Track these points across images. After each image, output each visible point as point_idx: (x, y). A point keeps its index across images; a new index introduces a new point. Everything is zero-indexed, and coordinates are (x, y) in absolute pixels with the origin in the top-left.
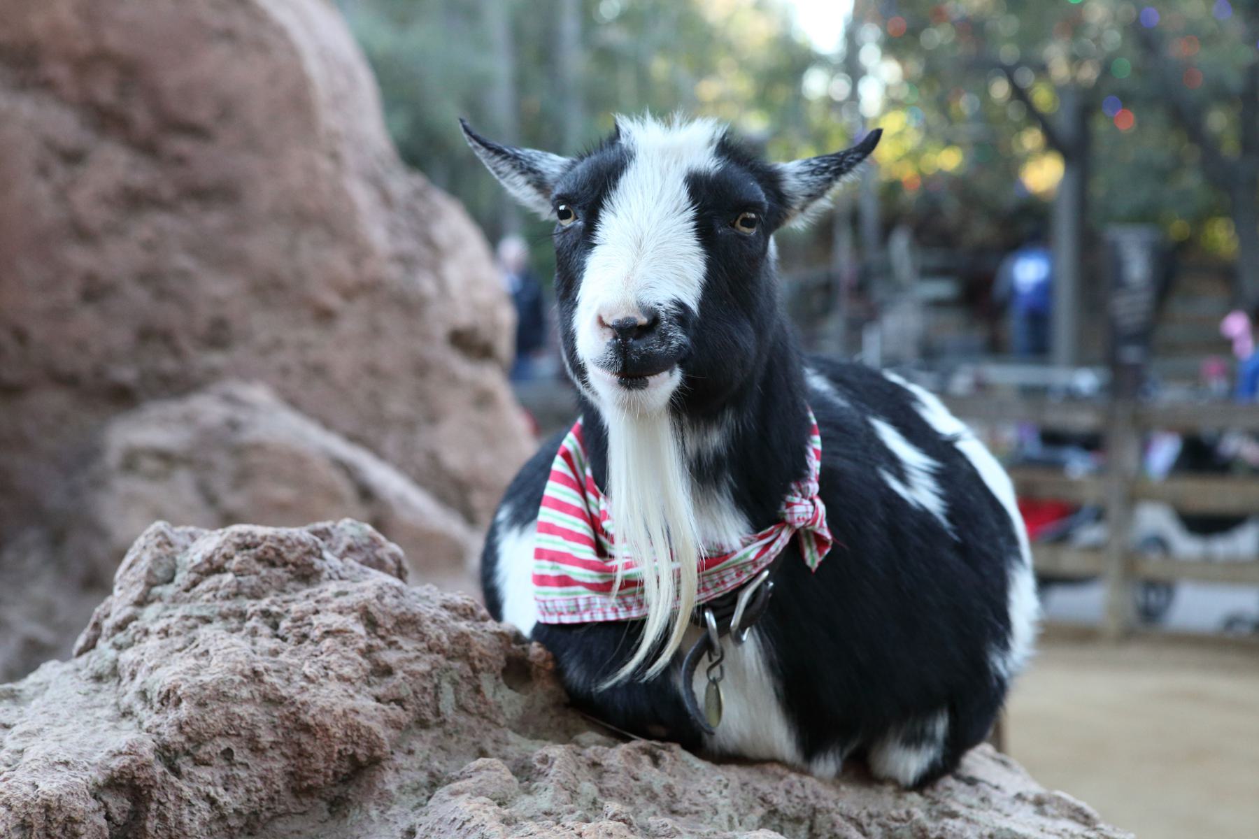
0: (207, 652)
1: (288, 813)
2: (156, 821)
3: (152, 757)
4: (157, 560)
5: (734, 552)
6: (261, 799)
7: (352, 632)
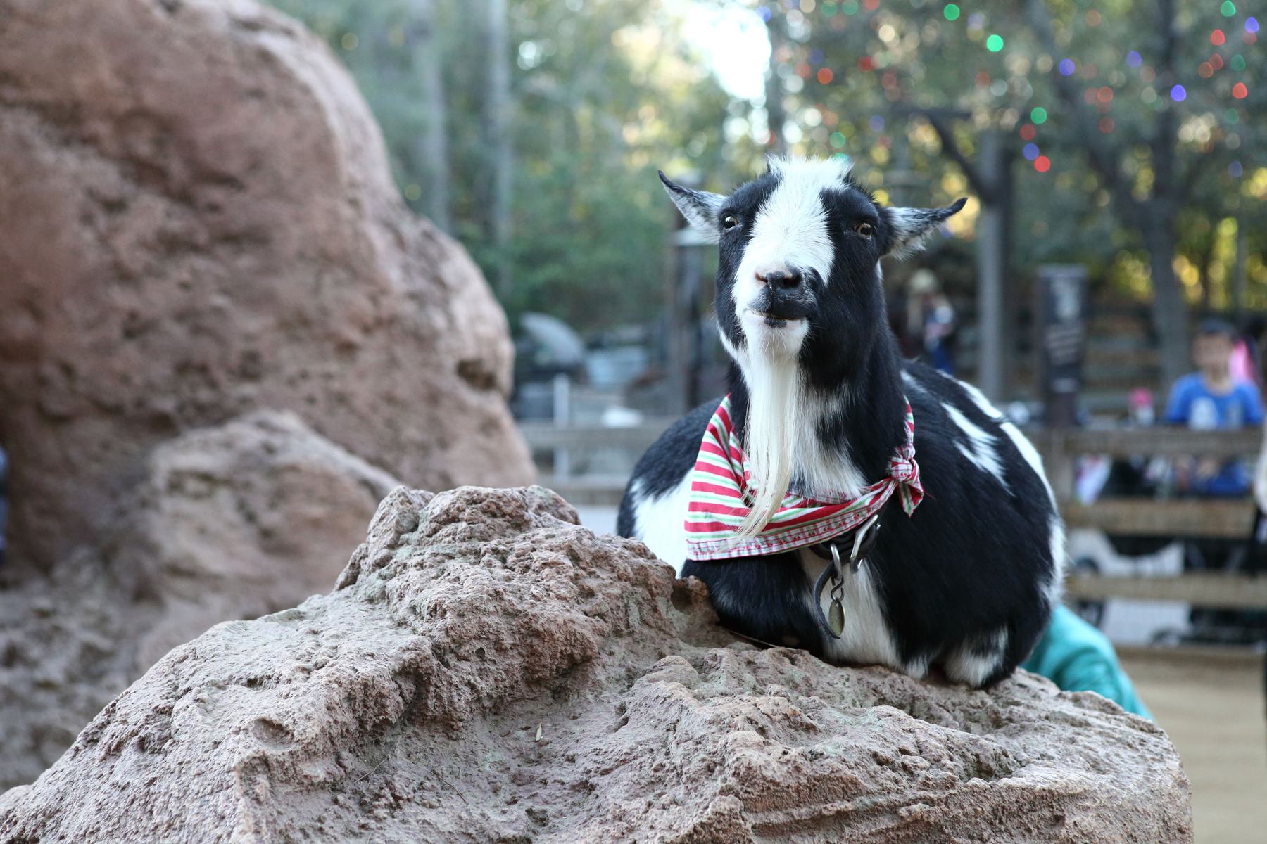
0: (458, 578)
1: (523, 698)
2: (434, 700)
3: (430, 652)
4: (402, 514)
5: (855, 499)
7: (564, 564)
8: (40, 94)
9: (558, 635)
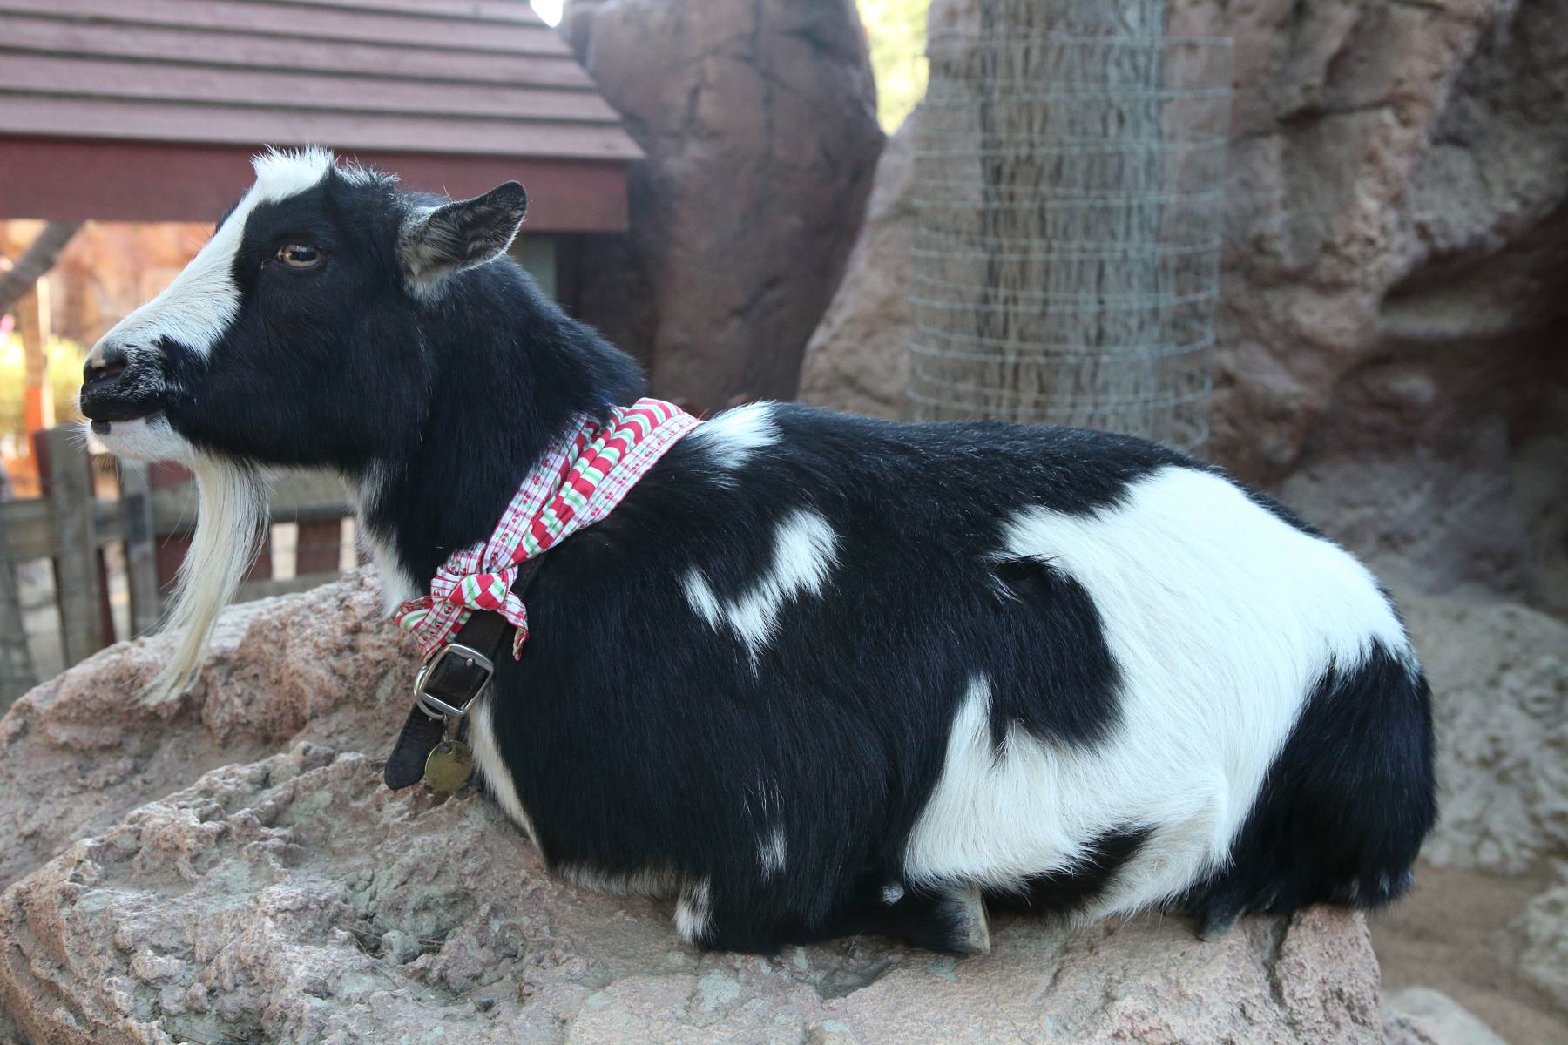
6: (266, 721)
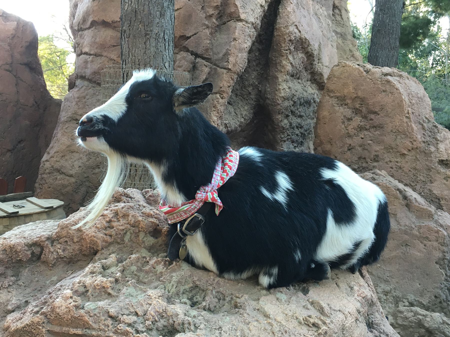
8: (338, 94)
9: (87, 240)
